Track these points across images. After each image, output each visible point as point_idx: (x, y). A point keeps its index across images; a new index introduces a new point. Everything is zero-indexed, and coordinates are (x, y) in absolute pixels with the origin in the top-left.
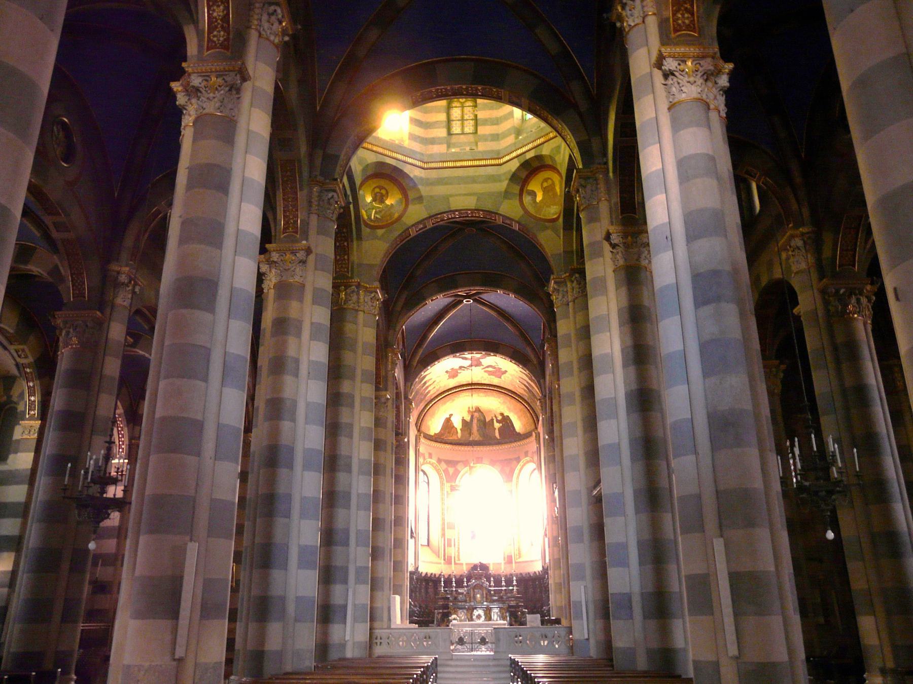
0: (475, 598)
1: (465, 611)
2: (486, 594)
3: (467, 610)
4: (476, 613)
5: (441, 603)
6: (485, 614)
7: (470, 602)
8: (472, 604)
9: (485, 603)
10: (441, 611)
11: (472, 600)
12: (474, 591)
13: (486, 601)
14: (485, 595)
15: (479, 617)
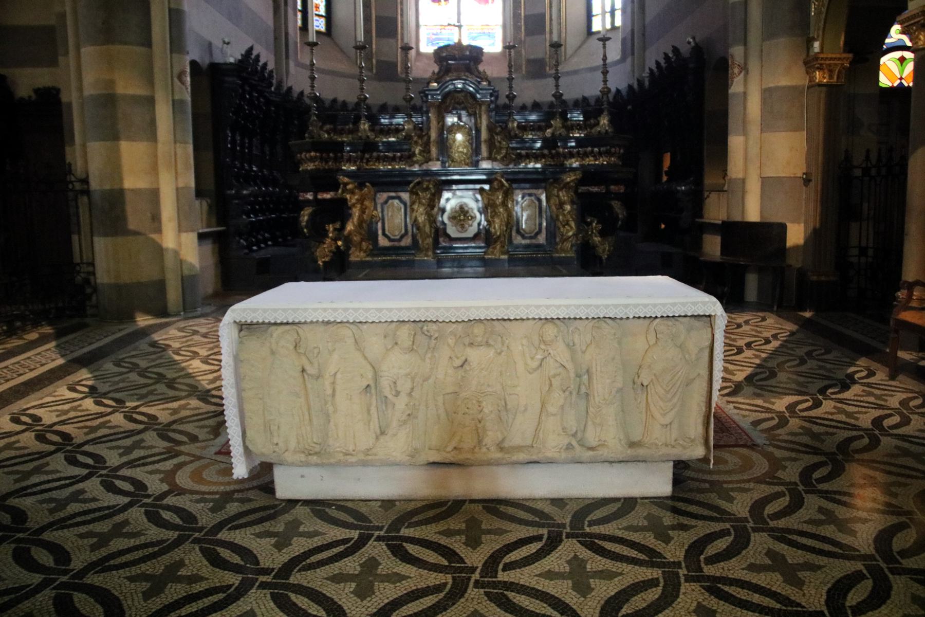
0: (444, 146)
1: (405, 196)
2: (491, 129)
3: (412, 193)
4: (450, 200)
5: (311, 166)
6: (488, 208)
7: (428, 160)
8: (436, 166)
9: (485, 165)
10: (310, 196)
11: (434, 151)
12: (441, 119)
13: (490, 158)
14: (484, 135)
15: (462, 214)
